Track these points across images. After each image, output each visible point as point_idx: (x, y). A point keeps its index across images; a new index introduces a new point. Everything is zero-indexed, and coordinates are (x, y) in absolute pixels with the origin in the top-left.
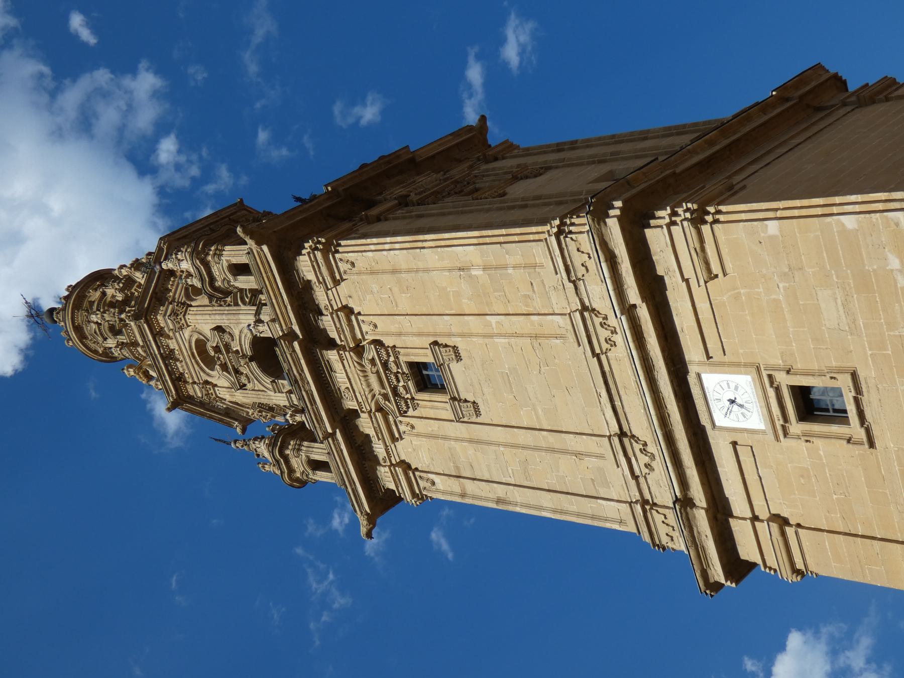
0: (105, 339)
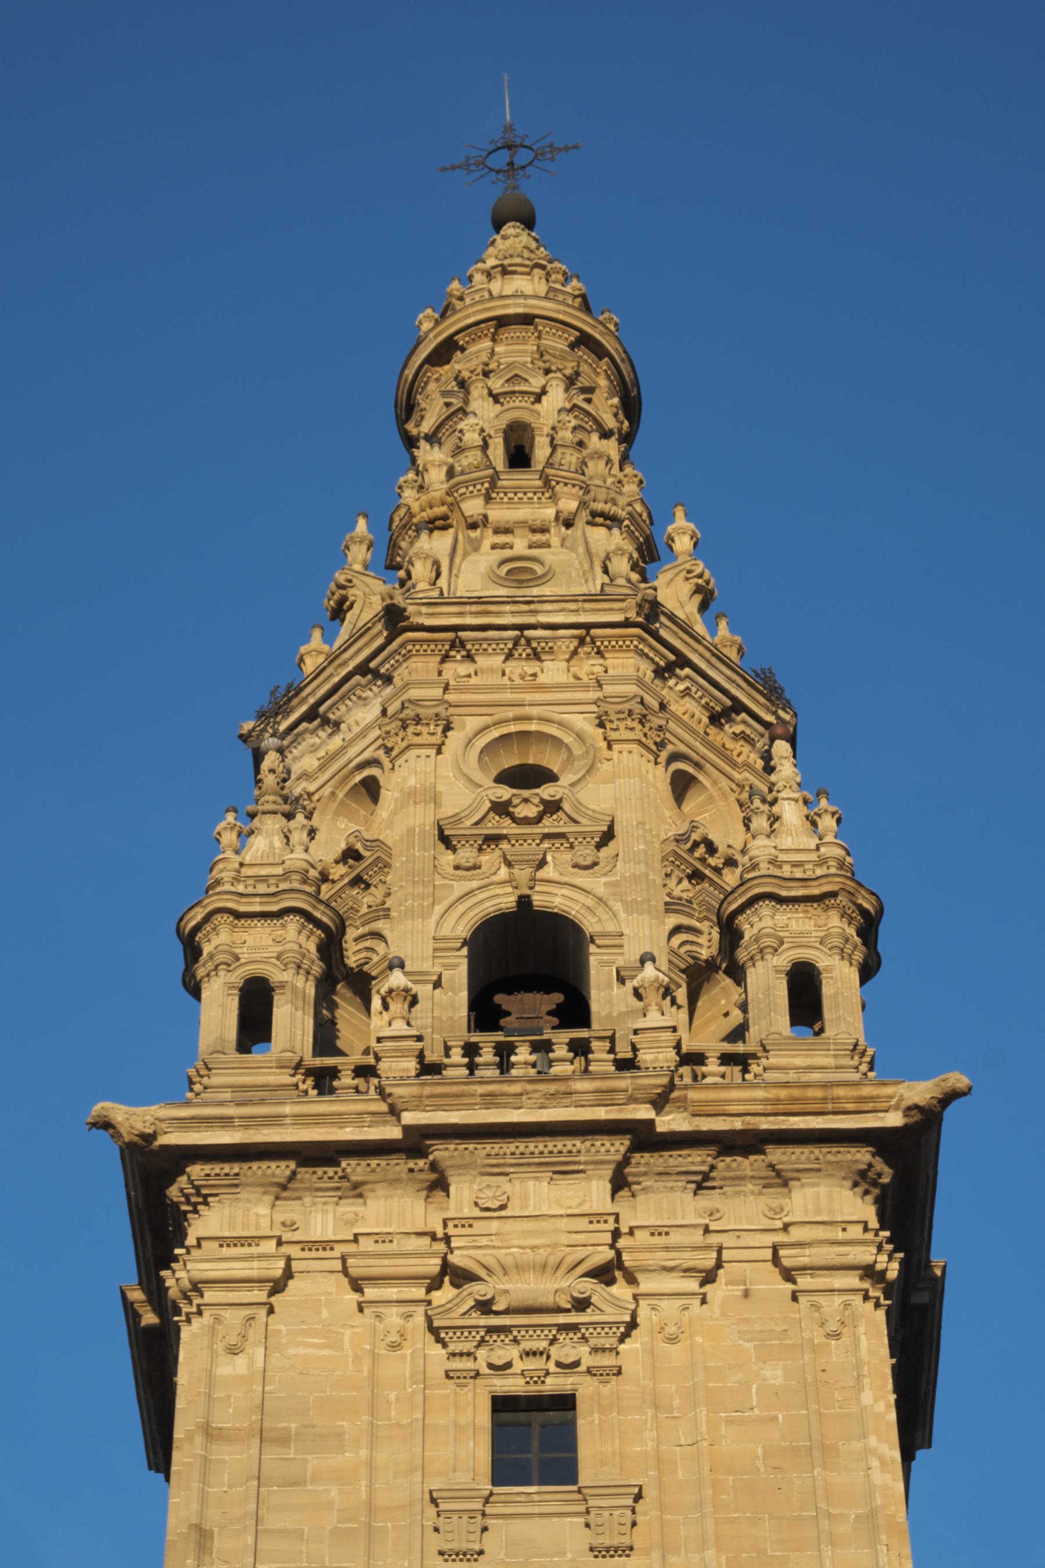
0: (496, 398)
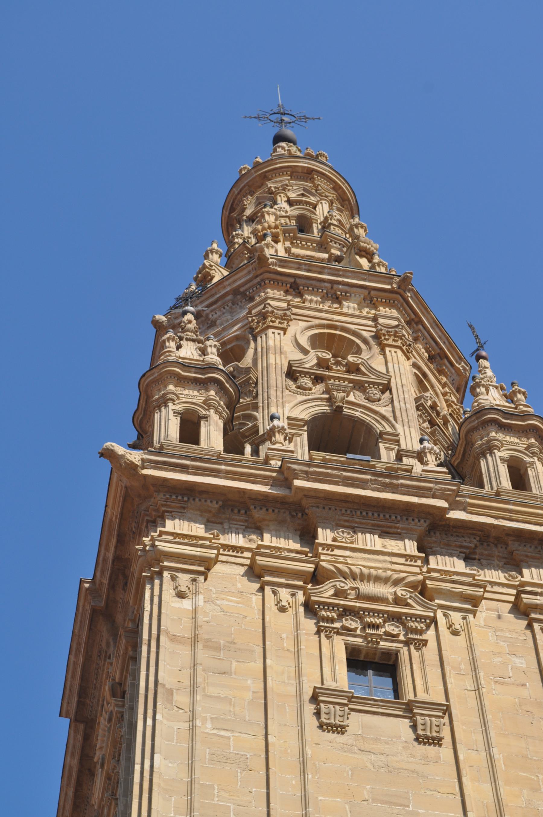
0: (290, 202)
